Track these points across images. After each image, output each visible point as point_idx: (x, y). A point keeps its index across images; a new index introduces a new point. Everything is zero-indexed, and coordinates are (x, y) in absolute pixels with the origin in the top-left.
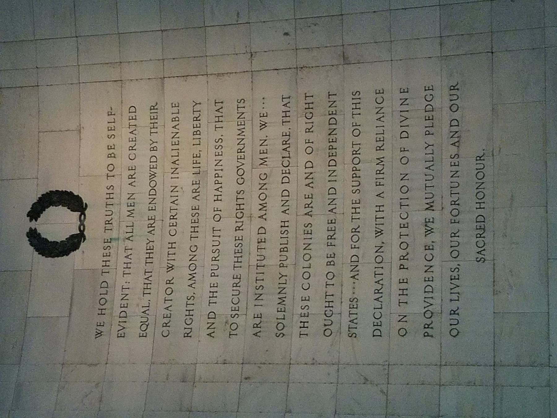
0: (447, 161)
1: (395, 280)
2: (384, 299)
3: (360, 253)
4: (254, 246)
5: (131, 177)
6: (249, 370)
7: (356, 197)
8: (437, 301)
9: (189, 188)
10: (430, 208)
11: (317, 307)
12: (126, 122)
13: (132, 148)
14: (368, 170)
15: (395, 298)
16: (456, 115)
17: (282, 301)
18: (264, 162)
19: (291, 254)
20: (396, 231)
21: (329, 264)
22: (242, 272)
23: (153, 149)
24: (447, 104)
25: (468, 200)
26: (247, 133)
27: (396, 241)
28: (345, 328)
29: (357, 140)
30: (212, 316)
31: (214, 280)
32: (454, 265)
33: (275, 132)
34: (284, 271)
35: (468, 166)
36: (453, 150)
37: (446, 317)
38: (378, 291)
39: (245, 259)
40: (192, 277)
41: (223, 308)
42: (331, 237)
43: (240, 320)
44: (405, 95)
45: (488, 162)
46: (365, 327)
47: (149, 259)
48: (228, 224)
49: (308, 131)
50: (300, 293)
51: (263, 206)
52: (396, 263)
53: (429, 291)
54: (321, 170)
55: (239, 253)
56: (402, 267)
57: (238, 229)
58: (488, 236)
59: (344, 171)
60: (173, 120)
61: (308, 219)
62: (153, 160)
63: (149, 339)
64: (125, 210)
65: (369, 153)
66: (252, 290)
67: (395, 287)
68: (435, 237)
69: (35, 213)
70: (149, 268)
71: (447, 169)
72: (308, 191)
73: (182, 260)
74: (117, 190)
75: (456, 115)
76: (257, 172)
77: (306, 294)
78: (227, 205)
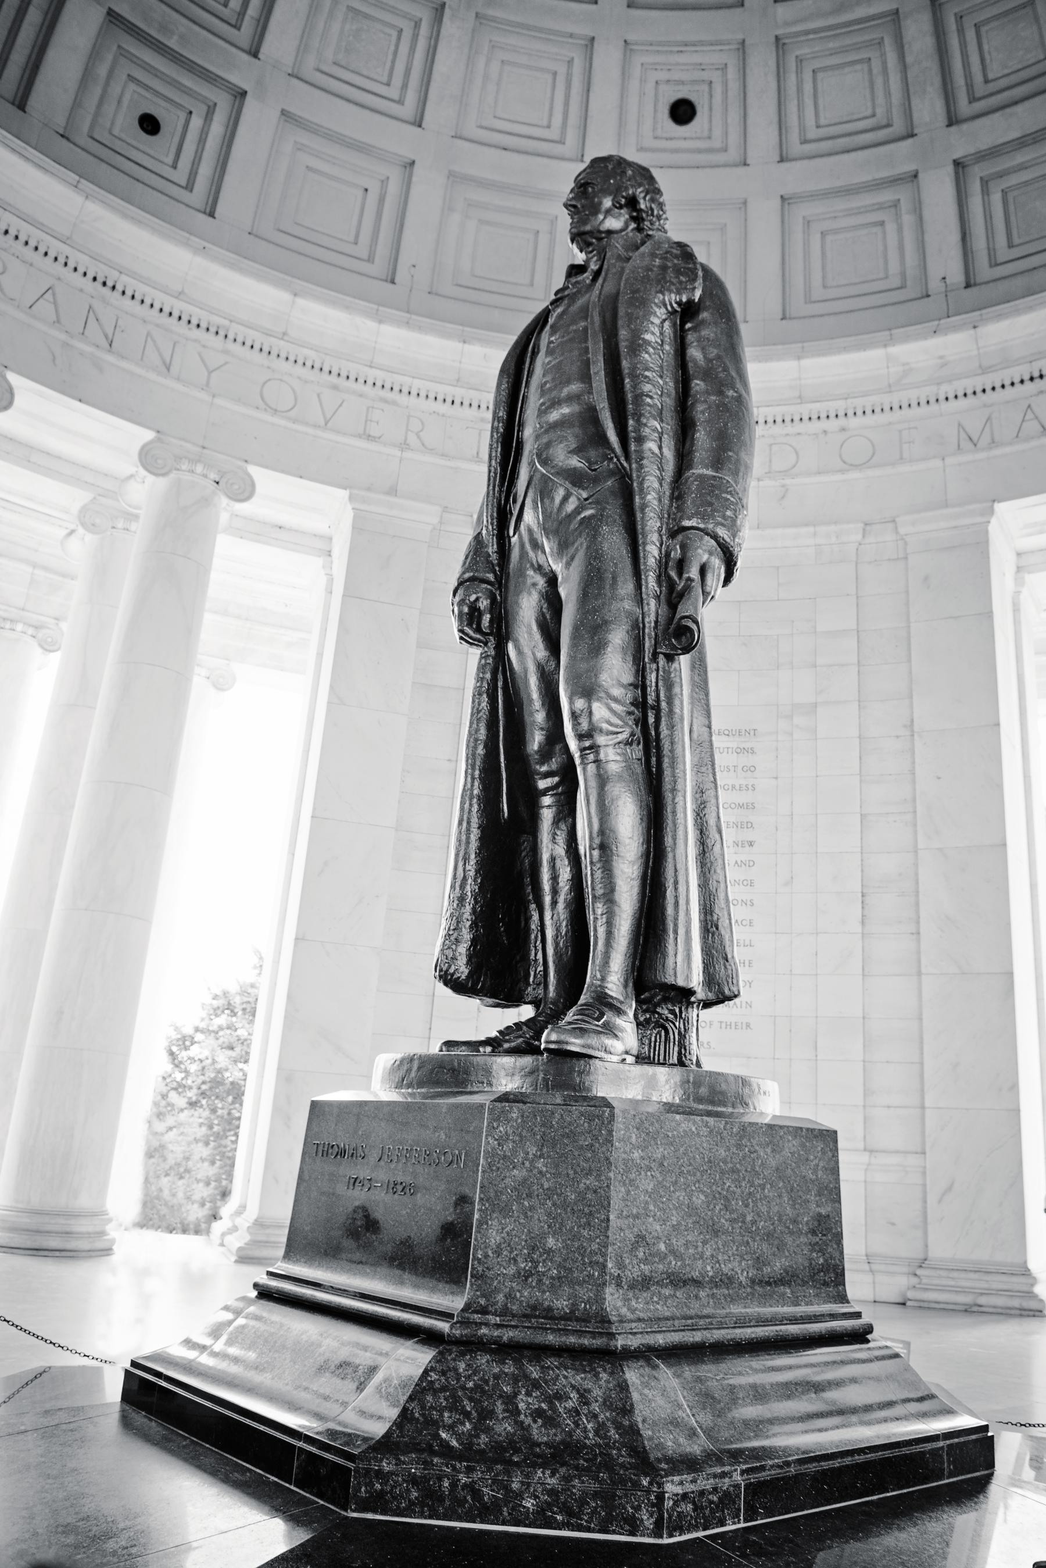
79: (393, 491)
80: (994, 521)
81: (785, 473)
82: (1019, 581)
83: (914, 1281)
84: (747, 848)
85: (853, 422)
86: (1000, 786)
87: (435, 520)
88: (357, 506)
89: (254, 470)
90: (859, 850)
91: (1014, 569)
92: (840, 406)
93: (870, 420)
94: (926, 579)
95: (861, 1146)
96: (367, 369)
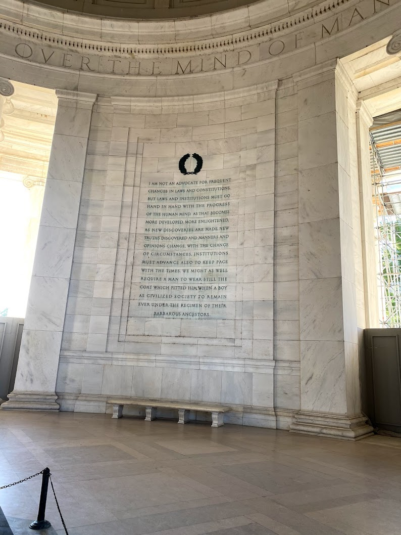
79: (76, 89)
80: (337, 67)
81: (246, 63)
82: (358, 104)
83: (294, 420)
84: (226, 230)
85: (275, 35)
86: (337, 191)
87: (94, 100)
88: (59, 96)
89: (13, 82)
90: (273, 226)
91: (355, 99)
92: (267, 27)
93: (282, 33)
94: (306, 100)
95: (272, 359)
96: (61, 36)
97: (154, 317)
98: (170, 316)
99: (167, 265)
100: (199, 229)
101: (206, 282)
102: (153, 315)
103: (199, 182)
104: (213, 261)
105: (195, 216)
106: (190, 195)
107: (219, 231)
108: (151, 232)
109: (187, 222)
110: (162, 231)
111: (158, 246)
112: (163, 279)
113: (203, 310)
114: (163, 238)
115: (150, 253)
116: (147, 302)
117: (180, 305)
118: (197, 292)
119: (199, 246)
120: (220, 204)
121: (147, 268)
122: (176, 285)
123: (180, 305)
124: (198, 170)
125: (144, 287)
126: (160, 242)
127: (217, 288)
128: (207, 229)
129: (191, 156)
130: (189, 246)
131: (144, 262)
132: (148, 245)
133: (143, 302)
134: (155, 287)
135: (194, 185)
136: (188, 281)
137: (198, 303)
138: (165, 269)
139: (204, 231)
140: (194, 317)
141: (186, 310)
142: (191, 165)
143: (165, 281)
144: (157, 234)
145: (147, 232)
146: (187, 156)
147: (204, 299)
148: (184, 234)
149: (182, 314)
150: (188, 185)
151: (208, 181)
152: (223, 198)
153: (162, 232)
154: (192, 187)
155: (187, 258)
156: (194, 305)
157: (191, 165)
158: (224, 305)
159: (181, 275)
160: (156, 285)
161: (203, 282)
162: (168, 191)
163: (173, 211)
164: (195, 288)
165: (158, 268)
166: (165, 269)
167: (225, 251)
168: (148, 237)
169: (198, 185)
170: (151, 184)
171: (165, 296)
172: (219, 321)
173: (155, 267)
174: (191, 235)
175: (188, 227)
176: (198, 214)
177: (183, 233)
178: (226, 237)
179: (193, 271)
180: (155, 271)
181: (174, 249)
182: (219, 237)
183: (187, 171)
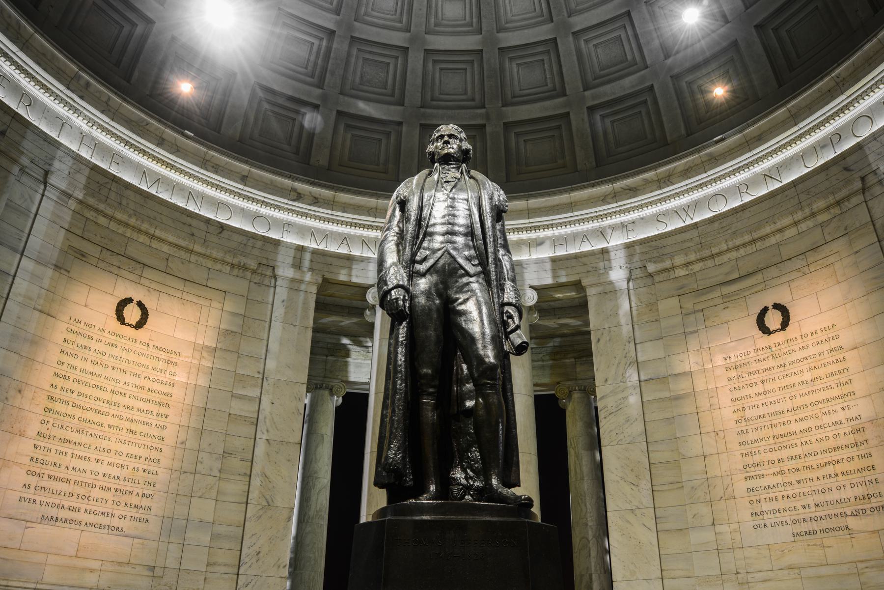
0: (842, 510)
1: (776, 494)
2: (766, 491)
3: (787, 474)
4: (781, 420)
5: (803, 347)
6: (721, 434)
7: (815, 466)
8: (769, 516)
9: (803, 379)
10: (816, 505)
11: (757, 458)
12: (830, 336)
13: (818, 343)
14: (830, 470)
15: (767, 496)
16: (868, 512)
17: (757, 441)
18: (825, 414)
19: (780, 440)
20: (801, 491)
21: (779, 460)
22: (767, 418)
23: (820, 354)
24: (874, 505)
25: (824, 524)
26: (838, 401)
27: (796, 491)
28: (748, 474)
29: (845, 460)
30: (744, 409)
31: (760, 405)
32: (789, 522)
33: (841, 416)
34: (771, 438)
35: (841, 522)
36: (849, 513)
37: (762, 522)
38: (769, 487)
39: (773, 418)
40: (760, 394)
41: (749, 413)
42: (792, 458)
43: (744, 423)
44: (874, 482)
45: (846, 532)
46: (751, 484)
47: (764, 370)
48: (789, 404)
49: (845, 434)
50: (762, 449)
51: (801, 420)
52: (785, 494)
53: (774, 512)
54: (825, 445)
55: (776, 414)
56: (783, 497)
57: (788, 410)
58: (808, 537)
59: (827, 457)
60: (837, 360)
61: (799, 444)
62: (814, 356)
63: (726, 383)
64: (787, 350)
65: (839, 468)
66: (759, 425)
67: (773, 495)
68: (802, 511)
69: (777, 306)
70: (761, 371)
71: (838, 511)
72: (814, 440)
73: (768, 386)
74: (795, 342)
75: (868, 512)
76: (818, 411)
77: (762, 452)
78: (799, 401)
97: (40, 523)
98: (66, 525)
99: (74, 447)
100: (128, 407)
101: (126, 483)
102: (39, 520)
103: (138, 342)
104: (140, 457)
105: (126, 387)
106: (124, 355)
107: (155, 417)
108: (58, 391)
109: (113, 392)
110: (75, 394)
111: (65, 415)
112: (63, 467)
113: (116, 522)
114: (74, 405)
115: (51, 421)
116: (33, 497)
117: (83, 510)
118: (108, 495)
119: (125, 431)
120: (162, 382)
121: (43, 444)
122: (81, 479)
123: (83, 510)
124: (140, 325)
125: (34, 474)
126: (70, 410)
127: (140, 494)
128: (139, 410)
129: (135, 302)
130: (110, 427)
131: (39, 434)
132: (50, 410)
133: (27, 496)
134: (50, 477)
135: (131, 343)
136: (100, 477)
137: (110, 511)
138: (70, 452)
139: (135, 411)
140: (102, 531)
141: (91, 518)
142: (132, 314)
143: (66, 471)
144: (67, 396)
145: (51, 389)
146: (128, 301)
147: (119, 508)
148: (104, 407)
149: (83, 523)
150: (123, 340)
151: (151, 346)
152: (168, 375)
153: (75, 395)
154: (129, 345)
155: (105, 444)
156: (103, 514)
157: (132, 314)
158: (147, 520)
159: (92, 466)
160: (52, 473)
161: (122, 482)
162: (95, 339)
163: (97, 369)
164: (110, 489)
165: (60, 448)
166: (70, 452)
167: (159, 446)
168: (52, 398)
169: (137, 345)
170: (73, 319)
171: (63, 493)
172: (136, 540)
173: (54, 446)
174: (115, 413)
175: (113, 400)
176: (131, 385)
177: (105, 405)
178: (164, 428)
179: (110, 464)
180: (53, 451)
181: (88, 425)
182: (154, 425)
183: (126, 321)
